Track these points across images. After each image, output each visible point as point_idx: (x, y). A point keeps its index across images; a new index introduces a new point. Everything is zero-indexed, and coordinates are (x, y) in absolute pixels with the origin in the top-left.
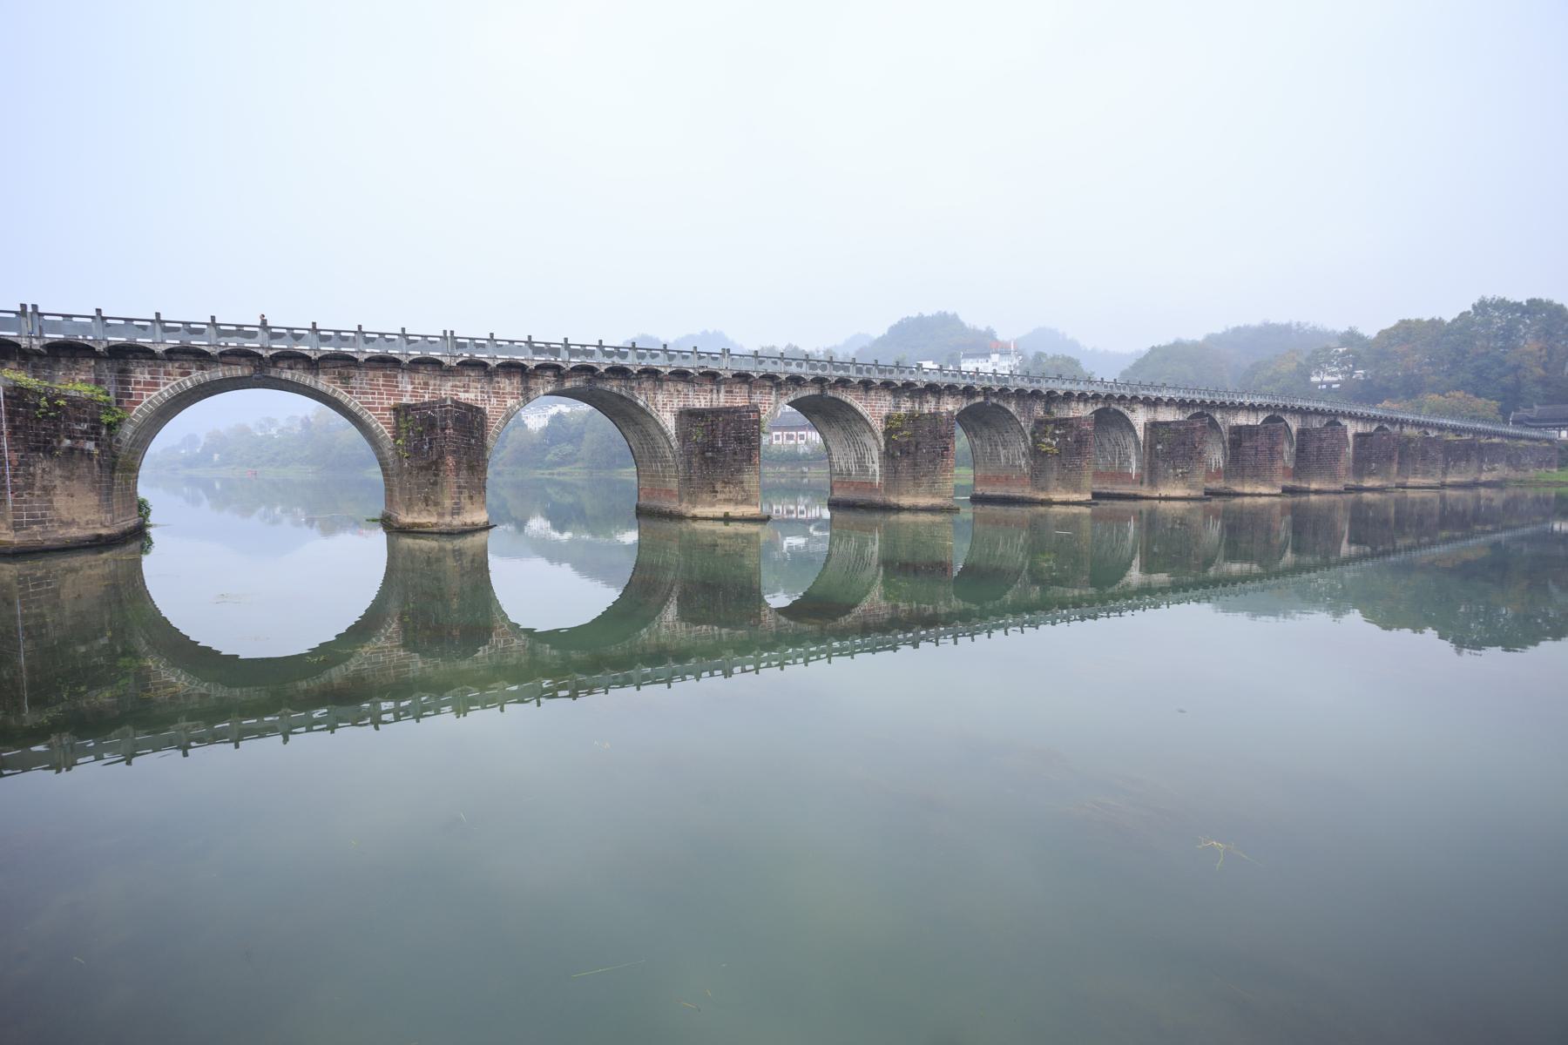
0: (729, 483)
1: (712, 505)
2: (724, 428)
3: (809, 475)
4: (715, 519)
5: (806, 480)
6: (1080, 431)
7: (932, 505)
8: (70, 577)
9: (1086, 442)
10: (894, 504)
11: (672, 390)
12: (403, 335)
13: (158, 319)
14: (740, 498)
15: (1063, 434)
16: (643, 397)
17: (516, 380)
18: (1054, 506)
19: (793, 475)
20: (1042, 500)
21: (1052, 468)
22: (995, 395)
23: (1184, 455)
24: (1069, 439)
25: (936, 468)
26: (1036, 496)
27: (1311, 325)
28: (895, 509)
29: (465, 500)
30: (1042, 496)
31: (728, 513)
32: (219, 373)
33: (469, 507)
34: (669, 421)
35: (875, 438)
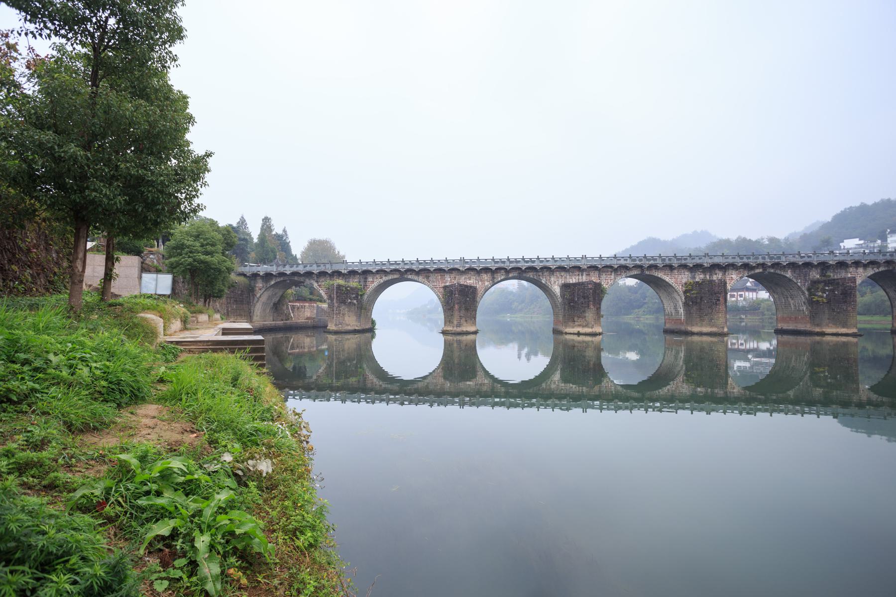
1: (573, 327)
3: (745, 320)
4: (574, 334)
5: (743, 324)
8: (348, 341)
11: (558, 275)
12: (446, 260)
13: (374, 261)
16: (544, 279)
17: (489, 275)
19: (733, 320)
20: (818, 332)
22: (769, 267)
24: (836, 292)
29: (463, 321)
30: (817, 330)
32: (390, 277)
33: (465, 324)
34: (557, 289)
35: (679, 295)
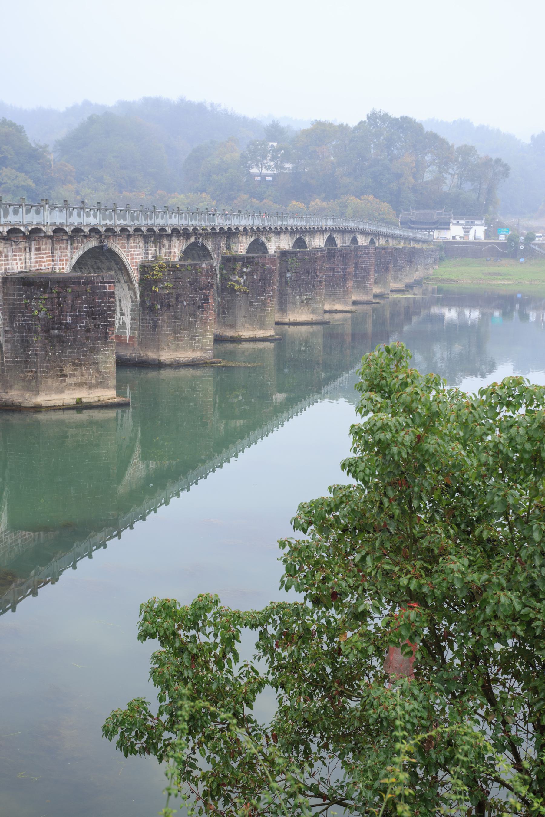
0: (81, 364)
1: (61, 391)
2: (73, 301)
4: (65, 408)
6: (265, 270)
7: (194, 358)
9: (270, 279)
10: (154, 360)
14: (94, 381)
15: (250, 272)
18: (243, 343)
20: (231, 337)
21: (240, 306)
23: (307, 283)
24: (255, 277)
25: (196, 321)
26: (225, 333)
27: (223, 107)
28: (156, 365)
31: (80, 399)
